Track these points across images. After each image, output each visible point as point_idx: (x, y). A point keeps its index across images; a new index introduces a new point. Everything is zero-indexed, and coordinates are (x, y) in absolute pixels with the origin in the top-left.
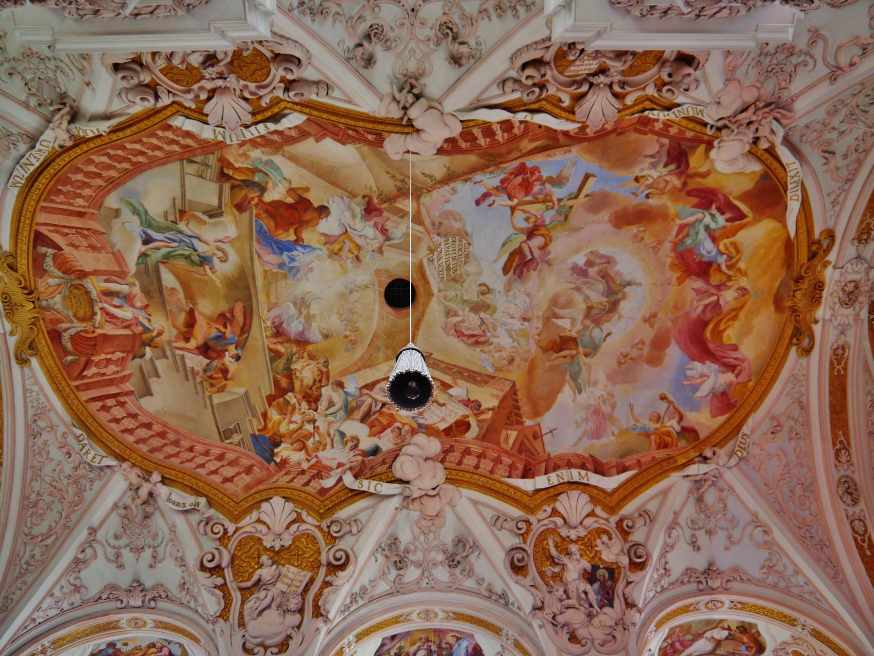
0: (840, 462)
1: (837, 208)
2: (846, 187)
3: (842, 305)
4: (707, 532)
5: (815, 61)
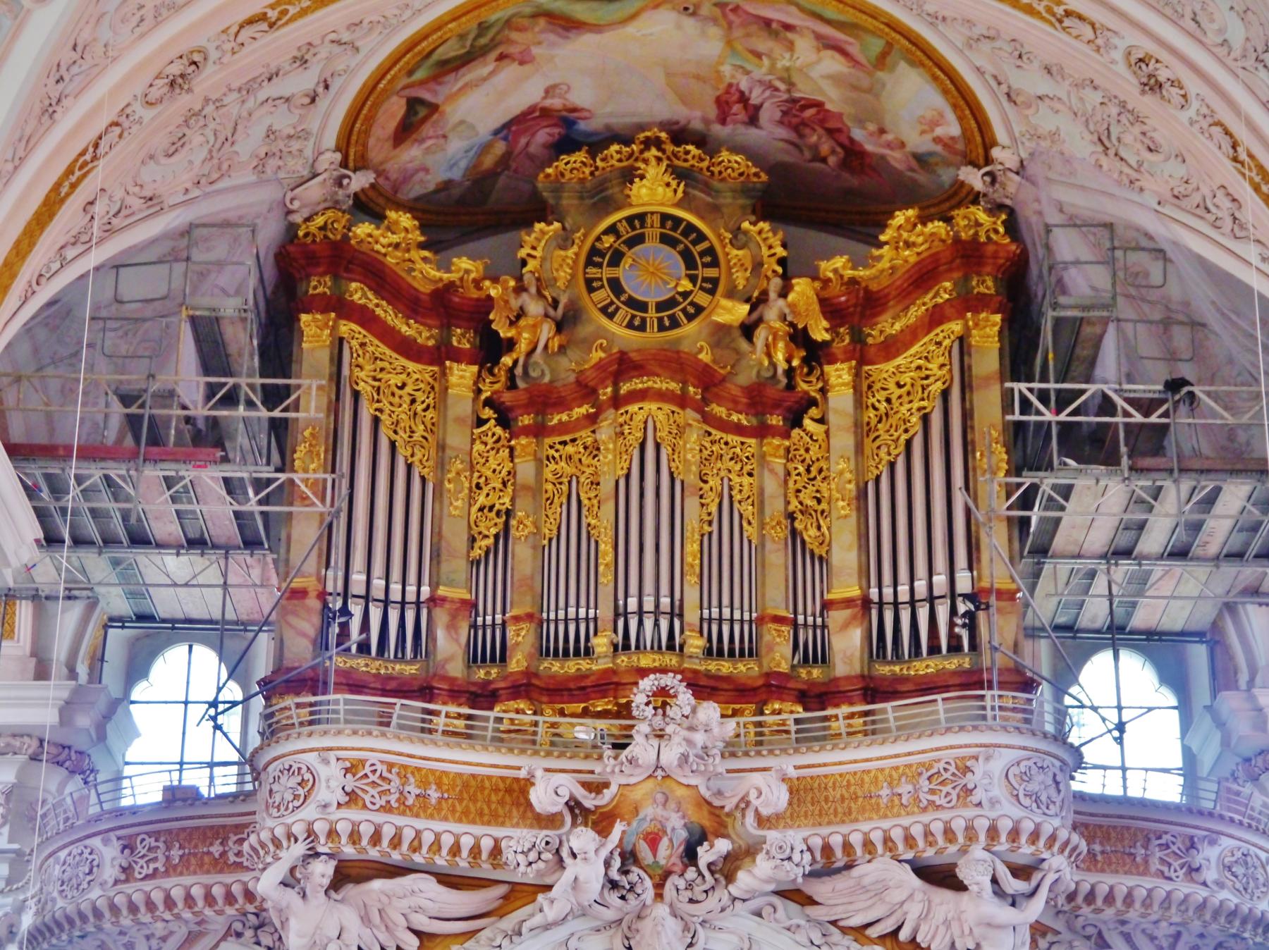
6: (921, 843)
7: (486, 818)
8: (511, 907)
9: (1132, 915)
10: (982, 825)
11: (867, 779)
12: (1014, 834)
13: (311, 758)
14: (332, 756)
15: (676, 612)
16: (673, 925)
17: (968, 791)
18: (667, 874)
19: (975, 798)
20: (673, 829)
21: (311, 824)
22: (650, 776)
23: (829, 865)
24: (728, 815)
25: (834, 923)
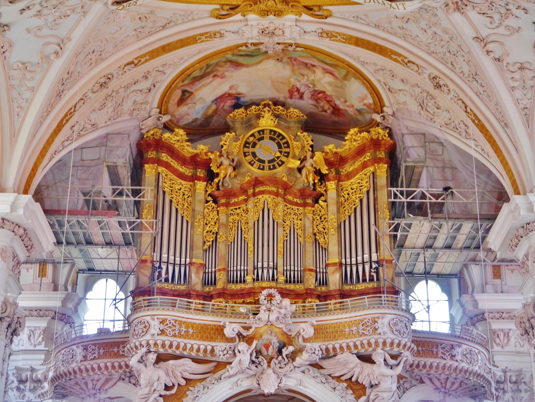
1: (351, 18)
4: (39, 11)
5: (494, 29)
6: (360, 347)
7: (209, 339)
8: (218, 370)
9: (432, 372)
10: (381, 341)
11: (341, 325)
12: (392, 344)
13: (148, 318)
14: (156, 317)
15: (275, 268)
16: (273, 376)
17: (376, 329)
18: (272, 358)
19: (378, 332)
21: (148, 341)
23: (328, 355)
24: (293, 338)
25: (330, 375)
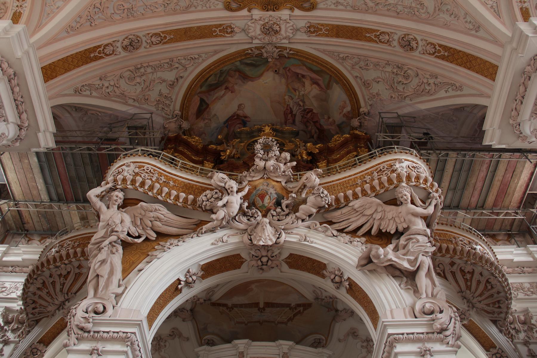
0: (152, 36)
1: (333, 7)
2: (349, 8)
3: (263, 25)
6: (378, 188)
16: (269, 230)
18: (268, 210)
20: (271, 193)
22: (261, 178)
